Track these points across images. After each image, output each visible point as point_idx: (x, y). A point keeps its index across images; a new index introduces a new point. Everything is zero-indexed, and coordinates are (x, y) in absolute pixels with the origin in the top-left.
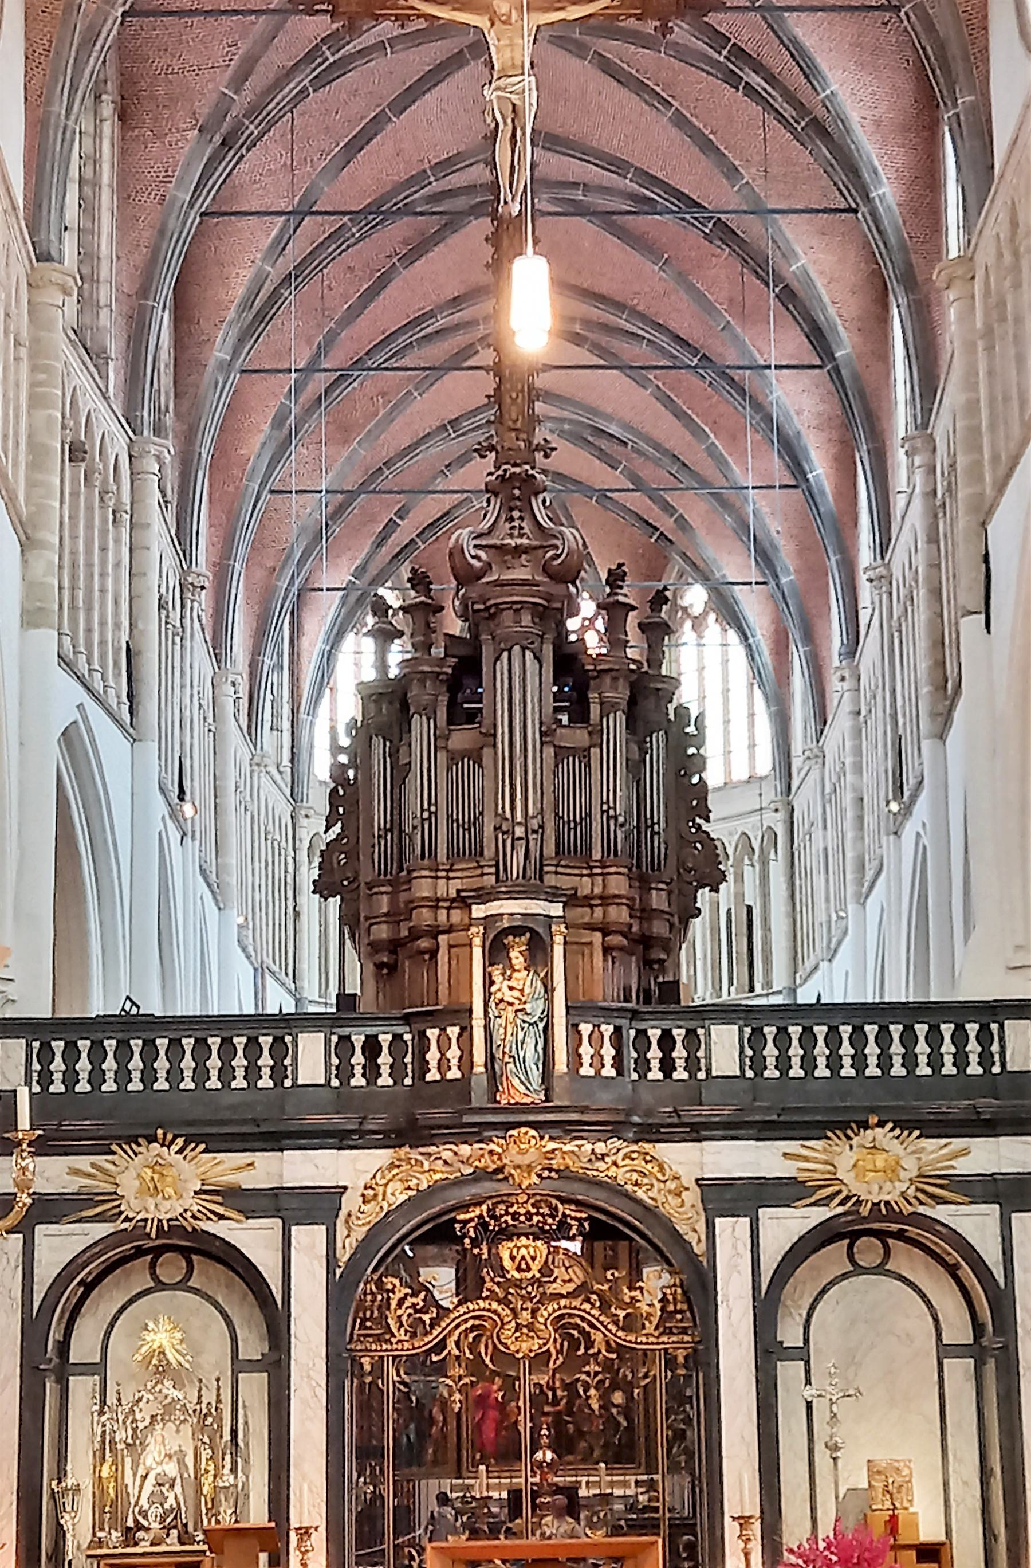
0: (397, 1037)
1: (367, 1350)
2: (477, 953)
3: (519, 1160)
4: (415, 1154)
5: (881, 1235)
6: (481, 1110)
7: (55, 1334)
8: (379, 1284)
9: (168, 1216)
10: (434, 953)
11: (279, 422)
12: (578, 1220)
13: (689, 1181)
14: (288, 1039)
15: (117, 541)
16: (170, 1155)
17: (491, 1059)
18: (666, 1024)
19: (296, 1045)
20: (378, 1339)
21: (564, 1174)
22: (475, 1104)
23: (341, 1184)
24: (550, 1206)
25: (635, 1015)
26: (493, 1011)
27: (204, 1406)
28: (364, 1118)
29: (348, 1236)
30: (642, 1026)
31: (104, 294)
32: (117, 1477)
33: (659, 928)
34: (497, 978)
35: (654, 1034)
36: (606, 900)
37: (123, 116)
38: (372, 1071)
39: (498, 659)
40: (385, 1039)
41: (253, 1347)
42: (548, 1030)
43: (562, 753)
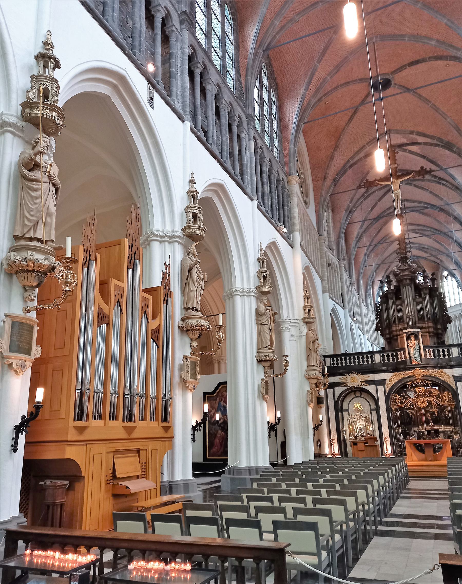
0: (392, 354)
2: (405, 339)
3: (417, 373)
4: (398, 373)
8: (394, 396)
10: (397, 339)
11: (365, 255)
13: (451, 376)
15: (338, 278)
16: (355, 375)
18: (443, 348)
19: (374, 356)
20: (395, 405)
21: (426, 376)
22: (408, 364)
24: (424, 381)
25: (436, 347)
26: (409, 348)
30: (438, 349)
31: (332, 239)
32: (353, 428)
33: (440, 331)
34: (409, 342)
35: (441, 350)
36: (429, 327)
37: (333, 211)
38: (388, 360)
39: (403, 288)
40: (390, 354)
41: (373, 406)
42: (420, 351)
43: (417, 303)
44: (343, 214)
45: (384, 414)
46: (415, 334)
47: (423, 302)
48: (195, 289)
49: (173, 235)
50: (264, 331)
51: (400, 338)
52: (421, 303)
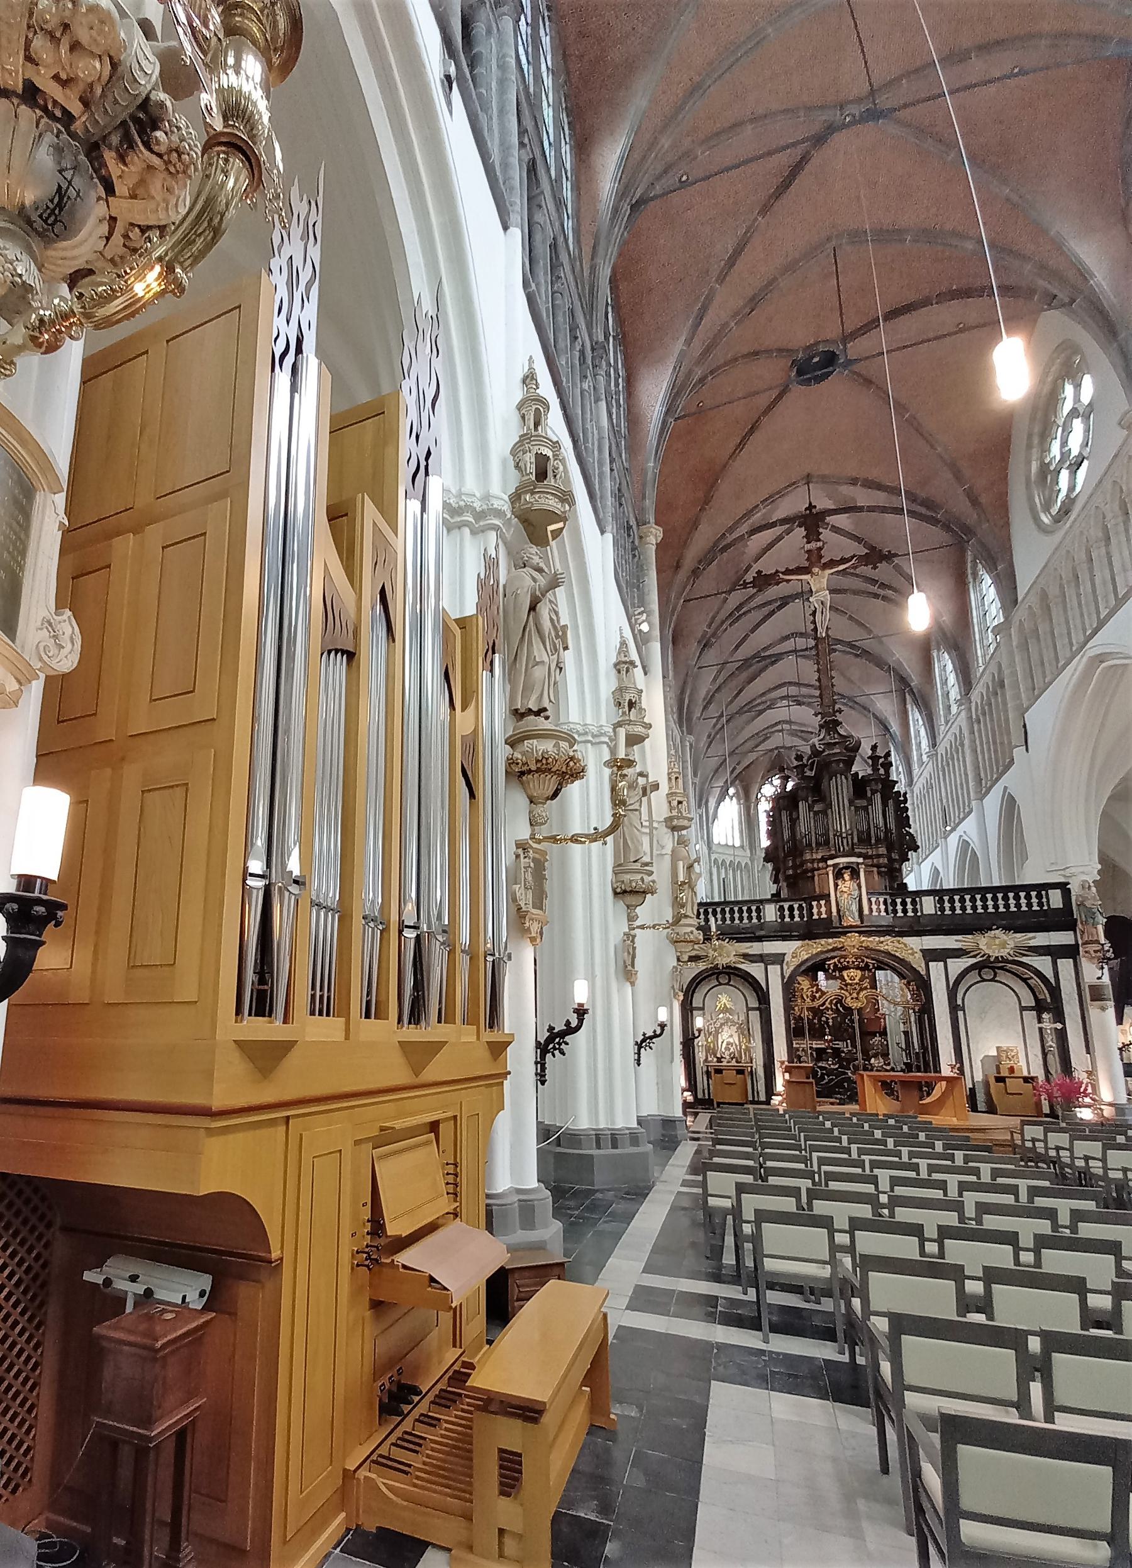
5: (993, 968)
6: (838, 928)
10: (813, 876)
11: (709, 736)
12: (873, 964)
17: (838, 911)
42: (860, 901)
44: (694, 647)
46: (852, 868)
47: (870, 807)
48: (546, 659)
49: (485, 507)
50: (631, 824)
51: (819, 875)
52: (866, 809)
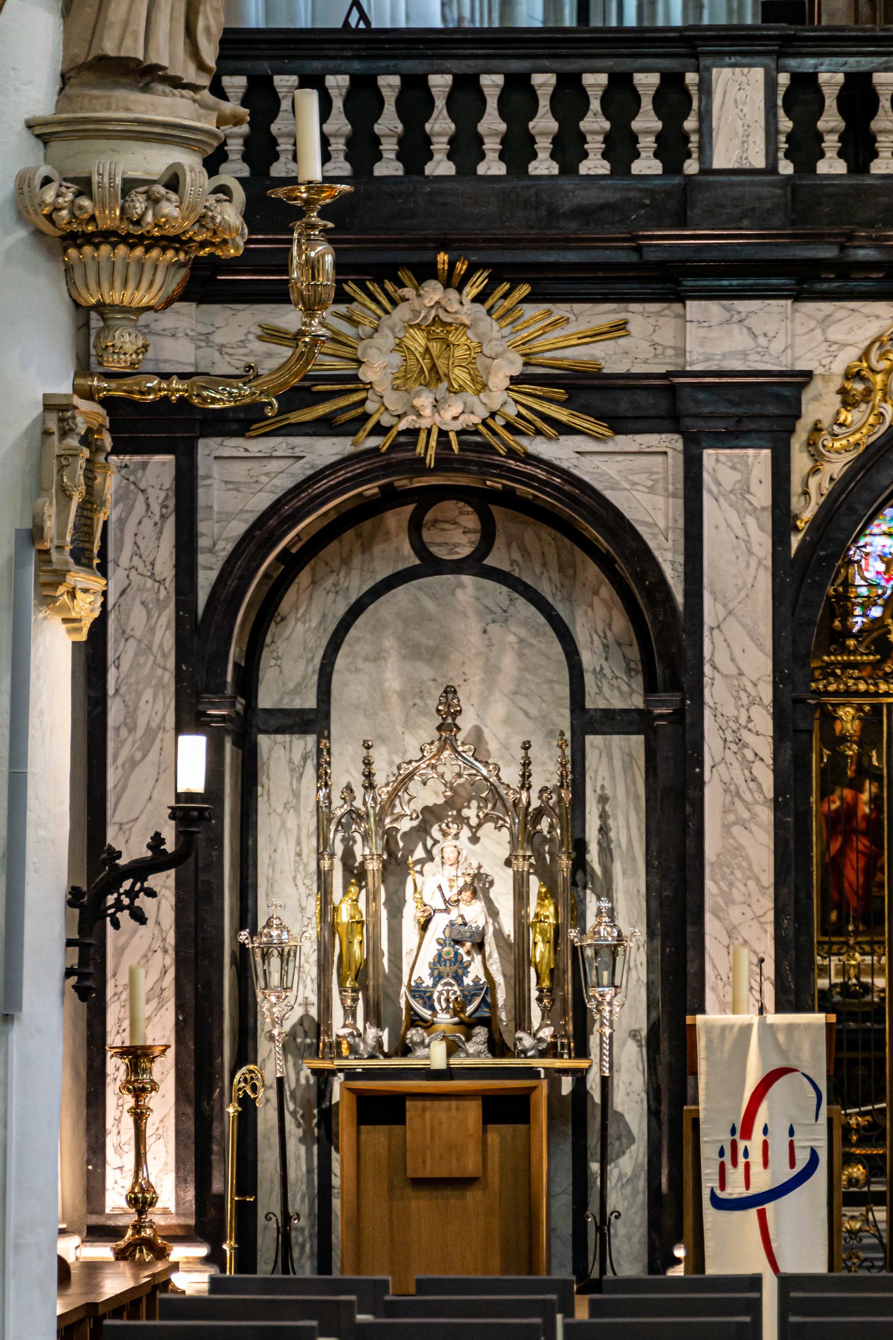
1: (848, 693)
7: (234, 653)
9: (458, 425)
14: (691, 78)
19: (706, 88)
23: (799, 367)
27: (534, 794)
28: (851, 237)
29: (815, 471)
45: (738, 774)
